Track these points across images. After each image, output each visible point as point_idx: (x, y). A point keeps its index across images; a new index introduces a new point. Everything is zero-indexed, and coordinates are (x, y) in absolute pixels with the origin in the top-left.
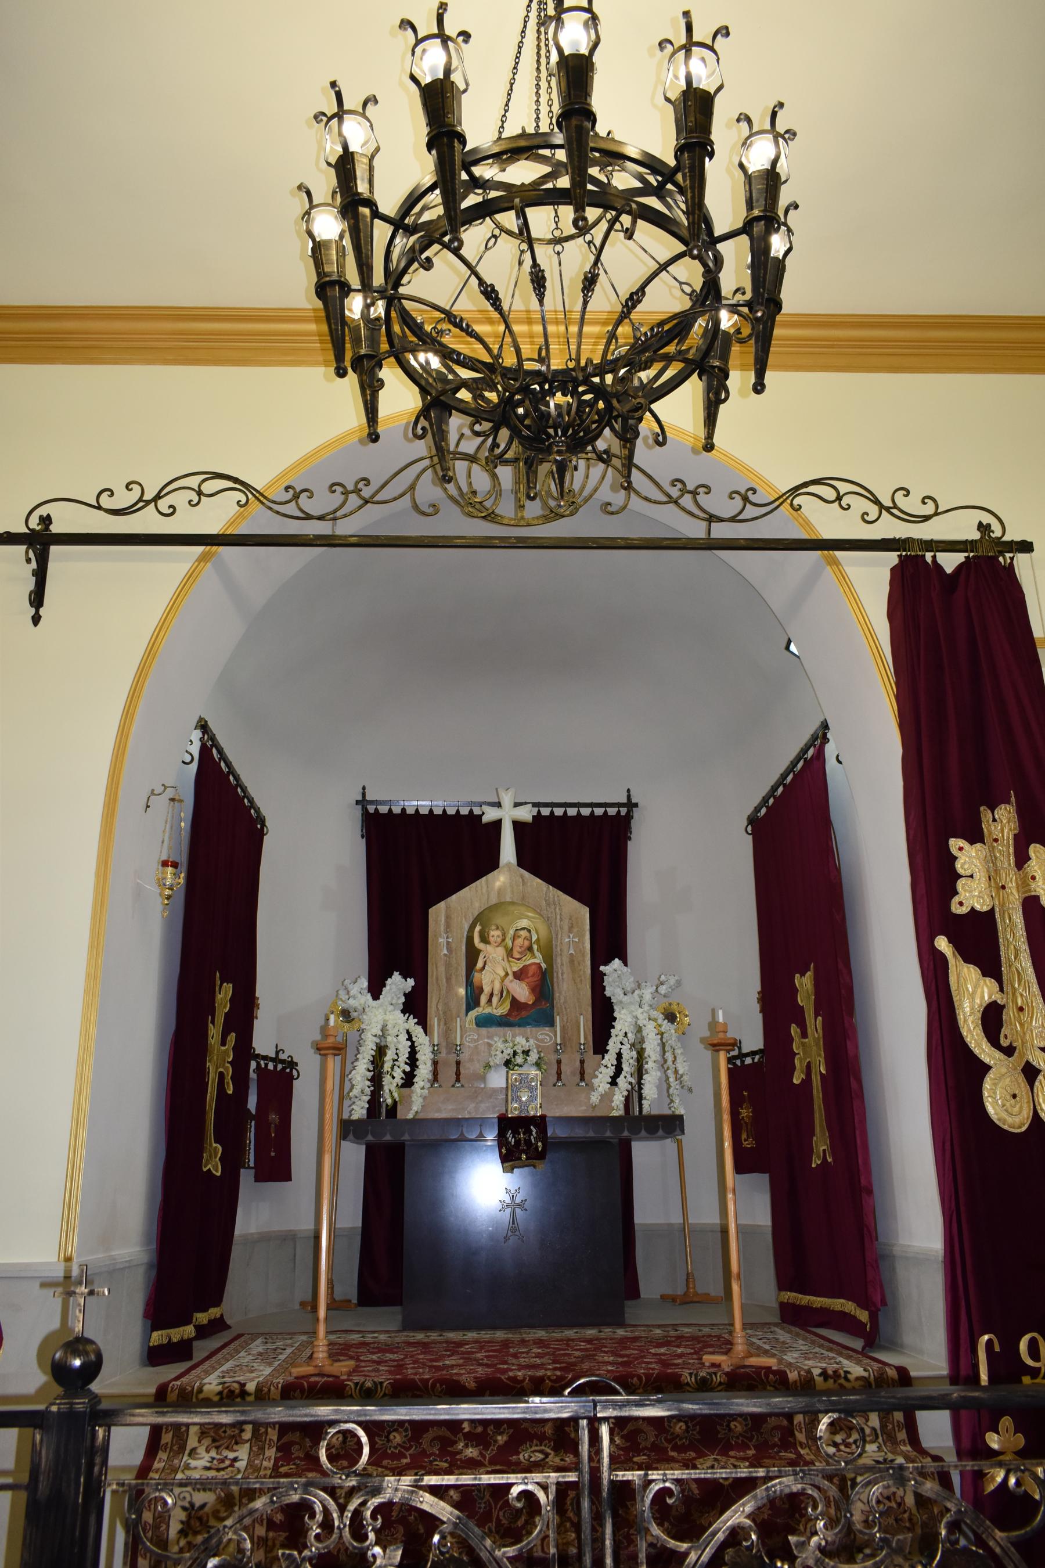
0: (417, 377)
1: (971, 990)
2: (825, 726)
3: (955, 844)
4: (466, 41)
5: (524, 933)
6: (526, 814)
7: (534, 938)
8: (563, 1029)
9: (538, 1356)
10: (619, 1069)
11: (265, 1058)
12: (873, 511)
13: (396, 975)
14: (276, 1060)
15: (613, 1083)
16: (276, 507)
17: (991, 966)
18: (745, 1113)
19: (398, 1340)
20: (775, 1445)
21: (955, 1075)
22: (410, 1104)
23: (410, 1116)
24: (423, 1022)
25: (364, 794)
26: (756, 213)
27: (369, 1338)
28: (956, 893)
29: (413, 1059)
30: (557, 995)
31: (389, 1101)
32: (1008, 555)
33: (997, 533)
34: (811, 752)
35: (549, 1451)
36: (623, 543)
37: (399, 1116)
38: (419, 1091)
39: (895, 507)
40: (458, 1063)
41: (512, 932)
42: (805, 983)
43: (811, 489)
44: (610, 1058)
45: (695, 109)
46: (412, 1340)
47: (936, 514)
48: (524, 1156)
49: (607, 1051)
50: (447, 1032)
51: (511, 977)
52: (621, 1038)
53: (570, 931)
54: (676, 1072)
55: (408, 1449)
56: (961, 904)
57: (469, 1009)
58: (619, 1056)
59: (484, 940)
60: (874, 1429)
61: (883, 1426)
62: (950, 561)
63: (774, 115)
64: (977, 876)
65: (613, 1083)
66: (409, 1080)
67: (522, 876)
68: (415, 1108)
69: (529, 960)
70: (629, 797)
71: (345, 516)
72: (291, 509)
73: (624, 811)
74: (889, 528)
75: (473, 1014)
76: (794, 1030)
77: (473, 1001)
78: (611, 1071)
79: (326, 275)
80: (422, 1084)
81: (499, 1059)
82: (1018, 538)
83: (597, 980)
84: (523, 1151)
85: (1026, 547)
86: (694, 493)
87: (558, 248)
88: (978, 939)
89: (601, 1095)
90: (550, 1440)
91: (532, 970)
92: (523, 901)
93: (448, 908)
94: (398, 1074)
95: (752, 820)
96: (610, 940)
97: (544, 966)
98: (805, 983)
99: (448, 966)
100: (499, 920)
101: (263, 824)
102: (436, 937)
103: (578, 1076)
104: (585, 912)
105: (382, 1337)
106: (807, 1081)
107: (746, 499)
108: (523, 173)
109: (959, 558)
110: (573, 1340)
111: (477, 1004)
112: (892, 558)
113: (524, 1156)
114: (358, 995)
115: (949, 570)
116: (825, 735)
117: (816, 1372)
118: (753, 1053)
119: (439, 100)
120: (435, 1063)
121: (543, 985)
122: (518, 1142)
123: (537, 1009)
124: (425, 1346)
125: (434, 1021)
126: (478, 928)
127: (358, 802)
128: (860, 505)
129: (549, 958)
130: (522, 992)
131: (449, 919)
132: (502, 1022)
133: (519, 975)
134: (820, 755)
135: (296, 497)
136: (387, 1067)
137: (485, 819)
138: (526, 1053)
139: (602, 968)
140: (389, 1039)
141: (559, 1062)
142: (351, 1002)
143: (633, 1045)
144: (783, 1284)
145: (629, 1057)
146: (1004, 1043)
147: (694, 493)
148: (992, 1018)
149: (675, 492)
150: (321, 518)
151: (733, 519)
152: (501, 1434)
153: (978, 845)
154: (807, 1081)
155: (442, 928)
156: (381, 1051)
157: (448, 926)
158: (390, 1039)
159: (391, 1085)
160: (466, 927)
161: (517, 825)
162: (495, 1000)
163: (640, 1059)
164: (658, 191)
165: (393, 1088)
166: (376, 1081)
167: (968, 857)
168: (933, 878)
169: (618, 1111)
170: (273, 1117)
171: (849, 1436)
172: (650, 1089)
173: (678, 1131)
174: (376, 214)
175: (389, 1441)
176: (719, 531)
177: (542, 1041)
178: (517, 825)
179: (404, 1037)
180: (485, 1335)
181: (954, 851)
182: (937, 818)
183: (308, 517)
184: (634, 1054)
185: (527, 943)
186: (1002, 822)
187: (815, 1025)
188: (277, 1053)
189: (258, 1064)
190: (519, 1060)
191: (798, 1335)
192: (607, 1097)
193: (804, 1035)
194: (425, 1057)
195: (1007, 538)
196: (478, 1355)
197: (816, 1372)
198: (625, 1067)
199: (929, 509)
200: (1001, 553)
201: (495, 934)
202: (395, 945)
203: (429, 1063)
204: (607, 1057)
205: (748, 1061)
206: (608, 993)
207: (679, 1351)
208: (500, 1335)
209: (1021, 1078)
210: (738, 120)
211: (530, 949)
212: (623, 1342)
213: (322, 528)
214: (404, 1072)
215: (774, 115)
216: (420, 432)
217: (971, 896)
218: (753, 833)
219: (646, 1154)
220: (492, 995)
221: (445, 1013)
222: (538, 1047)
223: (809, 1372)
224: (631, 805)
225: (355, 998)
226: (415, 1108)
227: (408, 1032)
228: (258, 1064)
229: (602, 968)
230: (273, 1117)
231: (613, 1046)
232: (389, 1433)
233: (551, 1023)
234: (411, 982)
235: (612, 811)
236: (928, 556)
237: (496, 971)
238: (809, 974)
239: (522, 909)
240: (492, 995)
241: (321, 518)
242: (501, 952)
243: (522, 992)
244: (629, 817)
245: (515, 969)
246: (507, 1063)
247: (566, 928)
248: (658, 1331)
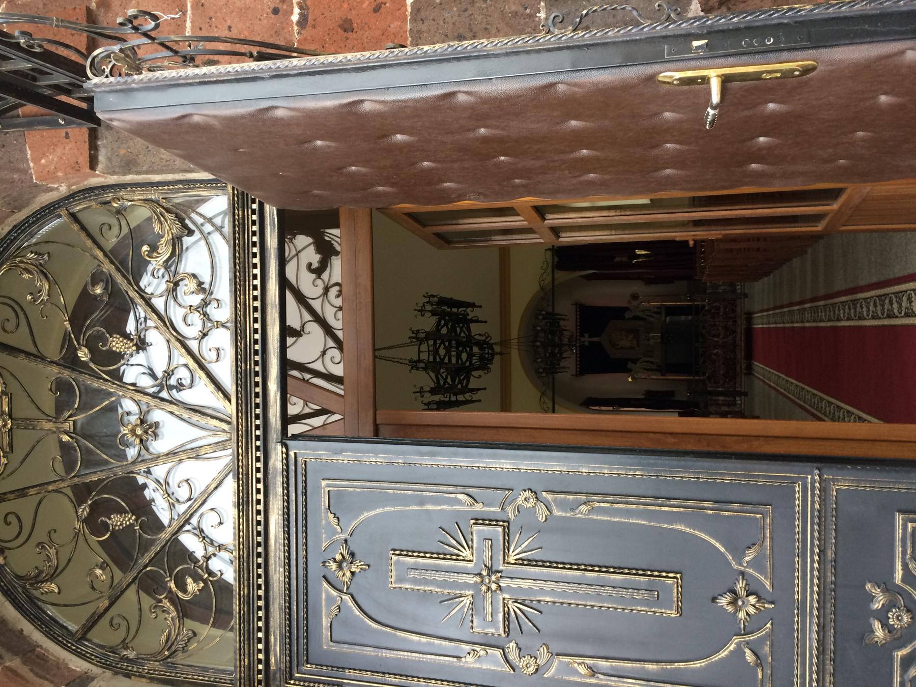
6: (586, 335)
24: (638, 359)
29: (647, 362)
62: (556, 259)
66: (652, 363)
74: (550, 269)
96: (618, 313)
128: (545, 276)
130: (631, 337)
159: (654, 367)
166: (652, 370)
202: (621, 366)
224: (576, 304)
243: (631, 337)
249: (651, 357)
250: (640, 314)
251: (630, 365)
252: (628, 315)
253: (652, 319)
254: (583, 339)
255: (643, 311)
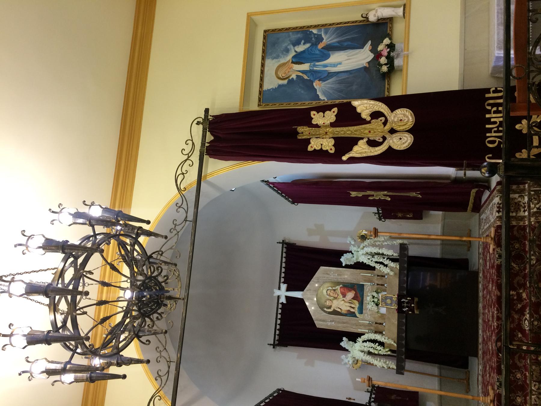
0: (128, 343)
1: (361, 149)
2: (263, 181)
3: (310, 149)
4: (13, 325)
5: (328, 292)
6: (284, 287)
7: (330, 288)
8: (366, 281)
9: (489, 311)
10: (381, 263)
11: (370, 398)
12: (188, 162)
13: (341, 344)
14: (371, 393)
15: (386, 266)
16: (163, 385)
17: (354, 141)
18: (400, 215)
19: (481, 362)
20: (524, 233)
21: (391, 157)
22: (390, 344)
23: (395, 345)
24: (360, 335)
25: (271, 345)
26: (88, 222)
27: (480, 373)
28: (327, 151)
30: (352, 282)
31: (389, 353)
32: (209, 117)
33: (201, 120)
34: (271, 185)
35: (524, 318)
36: (191, 254)
37: (396, 349)
38: (386, 340)
39: (188, 154)
40: (376, 323)
41: (328, 297)
42: (354, 194)
43: (179, 183)
44: (377, 266)
45: (50, 245)
46: (482, 357)
47: (192, 140)
48: (413, 305)
49: (374, 267)
50: (364, 325)
51: (344, 299)
52: (370, 261)
53: (329, 274)
54: (383, 241)
55: (523, 372)
56: (331, 149)
57: (356, 316)
58: (376, 262)
59: (330, 307)
60: (519, 196)
61: (518, 193)
62: (209, 137)
63: (53, 212)
64: (322, 143)
65: (386, 266)
66: (382, 344)
67: (307, 290)
68: (393, 343)
69: (339, 291)
70: (280, 243)
71: (169, 358)
72: (164, 378)
73: (285, 246)
74: (195, 158)
75: (358, 315)
76: (371, 198)
77: (353, 314)
78: (382, 266)
79: (87, 379)
80: (383, 339)
81: (375, 308)
82: (204, 113)
83: (347, 266)
84: (411, 305)
85: (207, 111)
86: (176, 225)
87: (86, 285)
88: (344, 145)
89: (391, 270)
90: (520, 317)
91: (342, 290)
92: (317, 290)
93: (317, 320)
94: (379, 348)
95: (293, 203)
97: (341, 286)
98: (354, 194)
99: (339, 322)
100: (323, 301)
101: (279, 390)
102: (327, 326)
103: (384, 278)
104: (322, 268)
105: (480, 367)
106: (390, 196)
107: (180, 207)
108: (63, 306)
109: (208, 134)
110: (483, 295)
111: (354, 313)
112: (206, 157)
113: (413, 305)
114: (347, 359)
115: (212, 138)
116: (266, 182)
117: (497, 214)
118: (378, 210)
119: (34, 339)
120: (376, 332)
121: (348, 287)
122: (407, 307)
123: (358, 290)
124: (484, 353)
125: (360, 331)
126: (325, 309)
127: (274, 348)
128: (186, 167)
129: (338, 283)
130: (350, 295)
131: (322, 321)
132: (361, 303)
133: (344, 295)
134: (273, 183)
135: (160, 376)
136: (376, 352)
137: (285, 302)
138: (373, 297)
139: (343, 265)
140: (365, 350)
141: (378, 284)
142: (350, 363)
143: (373, 256)
144: (465, 210)
145: (376, 258)
146: (381, 140)
147: (176, 225)
148: (372, 143)
149: (175, 232)
150: (169, 367)
151: (187, 212)
152: (518, 335)
153: (311, 141)
154: (390, 196)
155: (325, 323)
156: (370, 353)
157: (324, 321)
158: (366, 349)
160: (325, 314)
161: (288, 290)
162: (353, 306)
163: (378, 254)
164: (76, 258)
165: (385, 351)
167: (315, 145)
168: (321, 156)
169: (395, 266)
170: (393, 397)
171: (521, 206)
172: (390, 253)
173: (406, 246)
174: (69, 362)
175: (519, 379)
176: (191, 217)
177: (369, 289)
178: (288, 290)
179: (365, 344)
180: (480, 327)
181: (313, 149)
182: (299, 152)
183: (168, 372)
184: (376, 256)
185: (332, 291)
186: (304, 131)
187: (369, 193)
188: (368, 392)
189: (373, 402)
190: (376, 300)
191: (484, 211)
192: (392, 269)
193: (373, 196)
194: (373, 336)
195: (203, 117)
196: (488, 334)
197: (497, 214)
198: (381, 260)
199: (190, 143)
200: (208, 119)
201: (328, 303)
203: (376, 335)
204: (376, 267)
205: (381, 212)
206: (353, 264)
207: (488, 258)
208: (480, 321)
209: (394, 135)
210: (53, 224)
211: (334, 290)
212: (485, 277)
213: (173, 366)
214: (378, 345)
215: (53, 212)
216: (148, 342)
217: (328, 145)
218: (298, 203)
219: (413, 251)
220: (351, 307)
221: (357, 326)
222: (371, 292)
223: (497, 217)
224: (283, 243)
225: (349, 361)
226: (393, 343)
227: (363, 342)
228: (373, 402)
229: (343, 265)
230: (393, 397)
231: (373, 264)
232: (517, 378)
233: (363, 285)
234: (344, 339)
235: (285, 250)
236: (207, 145)
237: (343, 304)
238: (351, 192)
239: (319, 292)
240: (351, 307)
241: (169, 367)
242: (335, 302)
243: (350, 295)
244: (287, 244)
245: (342, 297)
246: (377, 305)
247: (327, 276)
248: (481, 261)
249: (381, 333)
250: (364, 259)
251: (345, 343)
252: (344, 260)
253: (386, 270)
254: (277, 293)
255: (373, 255)
